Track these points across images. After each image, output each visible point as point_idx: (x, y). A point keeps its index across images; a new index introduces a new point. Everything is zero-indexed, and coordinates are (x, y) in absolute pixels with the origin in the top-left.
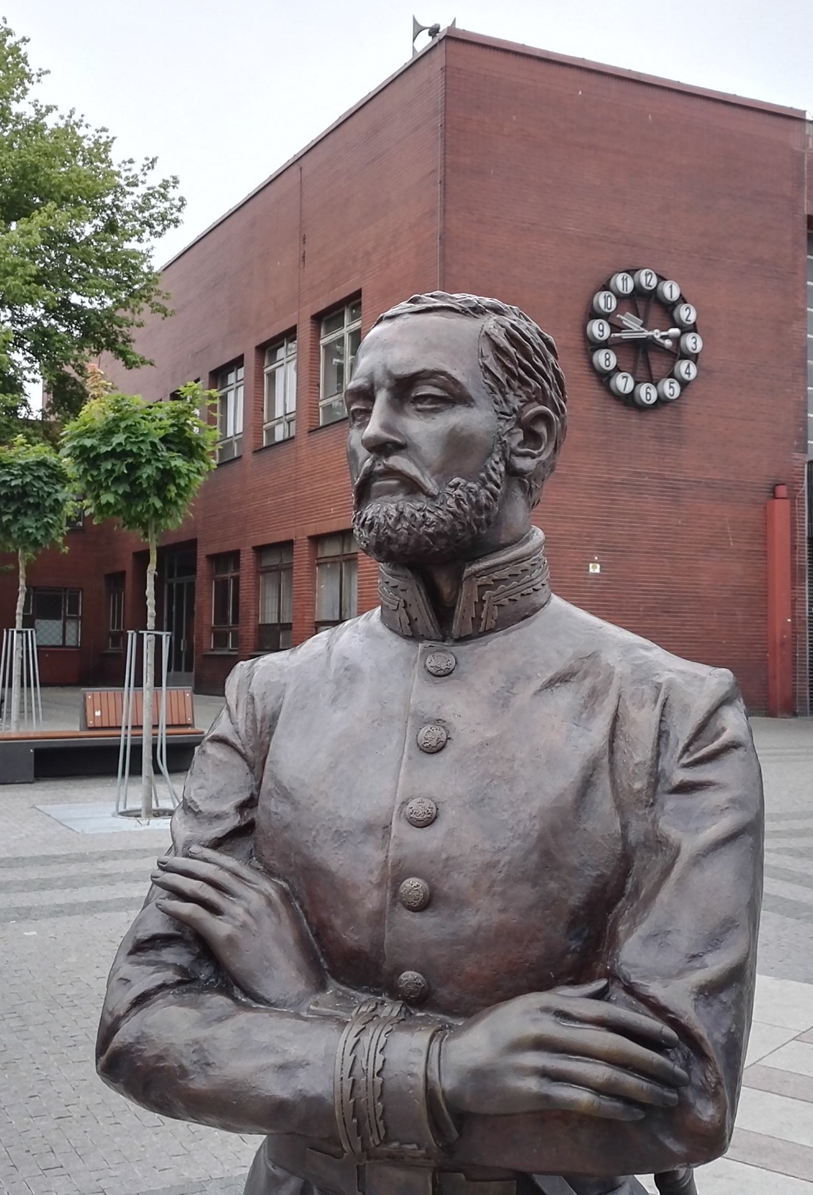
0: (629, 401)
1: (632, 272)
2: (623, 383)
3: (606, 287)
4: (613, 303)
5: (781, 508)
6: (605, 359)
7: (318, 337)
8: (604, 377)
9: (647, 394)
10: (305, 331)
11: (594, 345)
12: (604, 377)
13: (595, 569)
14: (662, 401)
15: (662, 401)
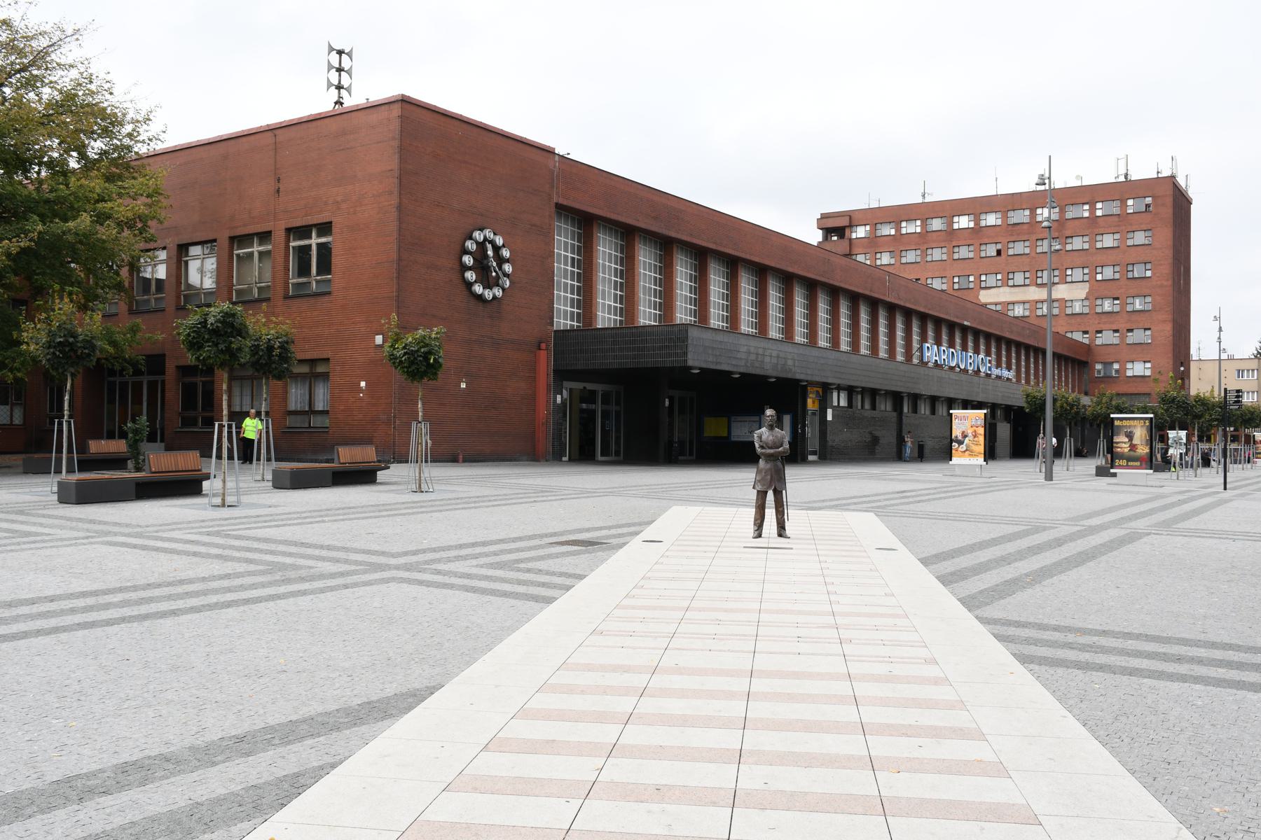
0: (480, 298)
1: (481, 230)
2: (478, 289)
3: (471, 238)
4: (475, 247)
5: (543, 354)
6: (471, 276)
7: (288, 241)
8: (469, 285)
9: (488, 294)
10: (279, 236)
11: (465, 268)
12: (469, 285)
13: (463, 386)
14: (495, 297)
15: (495, 297)
